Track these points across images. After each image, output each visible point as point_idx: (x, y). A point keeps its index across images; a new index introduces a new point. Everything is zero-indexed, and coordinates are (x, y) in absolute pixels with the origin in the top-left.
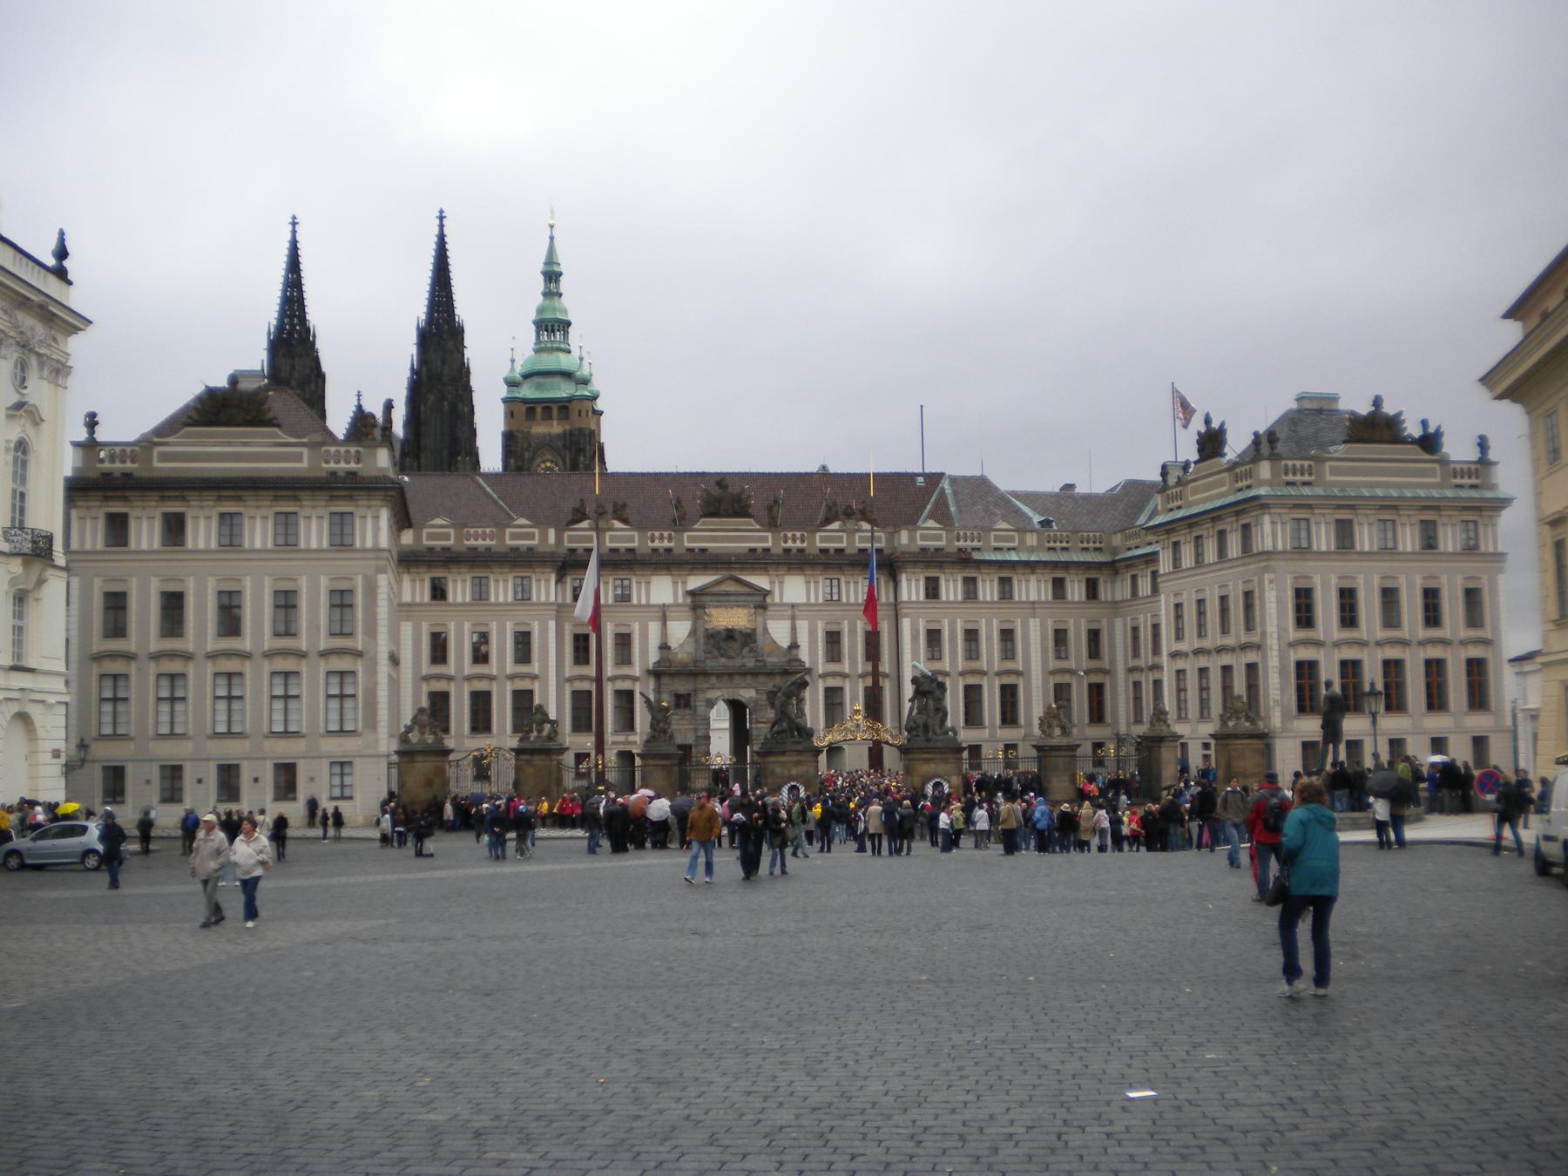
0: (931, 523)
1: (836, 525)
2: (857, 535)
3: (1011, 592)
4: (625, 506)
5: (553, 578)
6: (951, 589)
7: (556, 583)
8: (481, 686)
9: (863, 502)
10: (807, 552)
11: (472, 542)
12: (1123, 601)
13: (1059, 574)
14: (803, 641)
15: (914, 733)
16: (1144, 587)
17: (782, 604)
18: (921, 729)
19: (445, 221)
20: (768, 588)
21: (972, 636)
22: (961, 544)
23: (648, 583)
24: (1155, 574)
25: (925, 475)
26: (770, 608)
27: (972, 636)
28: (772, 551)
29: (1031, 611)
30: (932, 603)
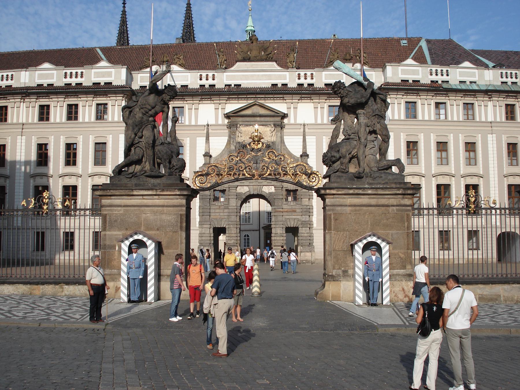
3: (473, 115)
8: (70, 181)
10: (315, 86)
11: (68, 80)
13: (511, 101)
14: (311, 151)
15: (337, 165)
20: (286, 113)
21: (442, 146)
22: (434, 78)
25: (409, 40)
26: (286, 127)
27: (442, 146)
28: (289, 86)
29: (490, 129)
30: (412, 122)
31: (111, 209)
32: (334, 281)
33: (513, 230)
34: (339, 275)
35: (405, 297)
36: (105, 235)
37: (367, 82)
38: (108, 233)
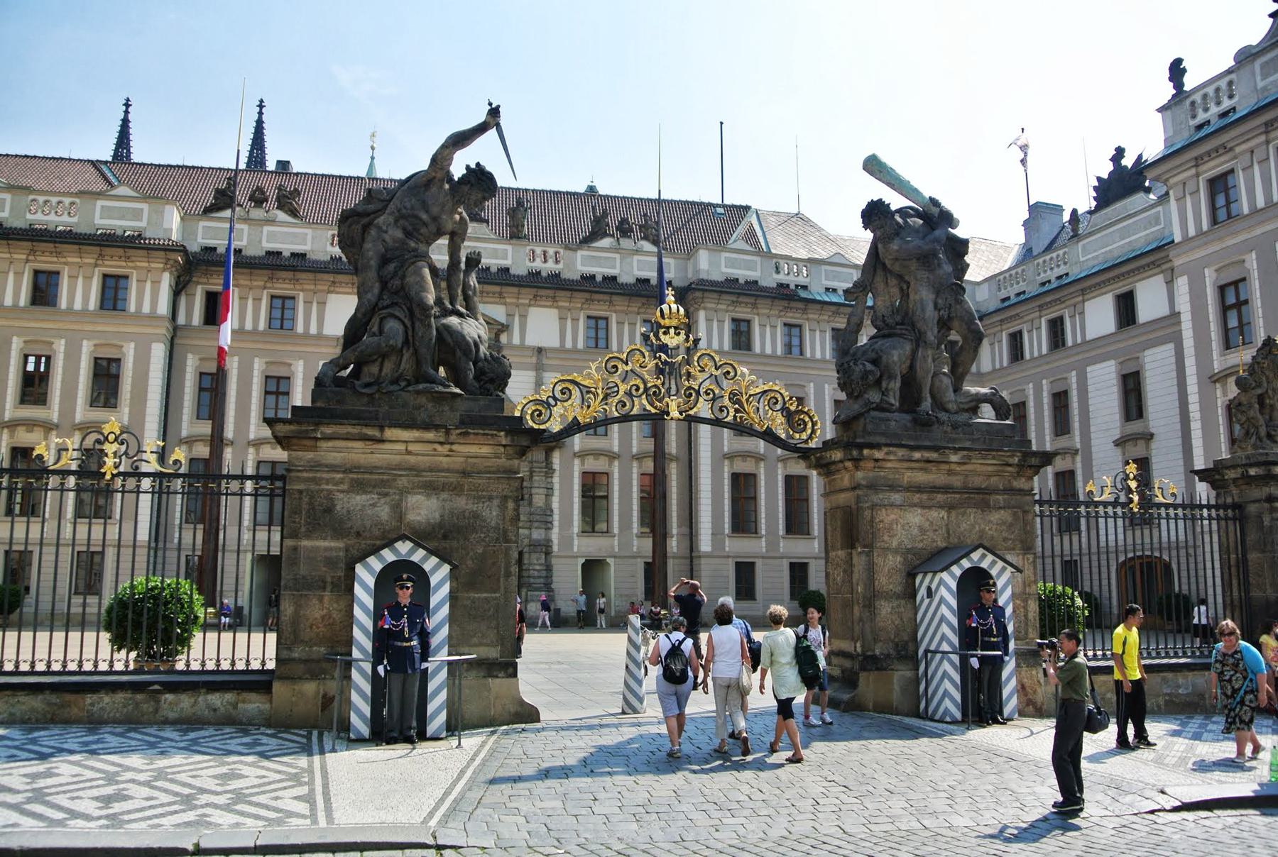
0: (742, 245)
1: (606, 242)
2: (636, 258)
4: (296, 192)
5: (166, 281)
6: (768, 338)
7: (177, 292)
9: (645, 215)
12: (994, 370)
15: (874, 396)
16: (1037, 342)
17: (522, 347)
18: (896, 385)
19: (264, 110)
22: (782, 278)
23: (322, 304)
24: (1056, 328)
31: (315, 478)
32: (877, 669)
33: (1157, 554)
34: (888, 656)
35: (1028, 705)
36: (295, 549)
37: (938, 210)
38: (305, 543)
